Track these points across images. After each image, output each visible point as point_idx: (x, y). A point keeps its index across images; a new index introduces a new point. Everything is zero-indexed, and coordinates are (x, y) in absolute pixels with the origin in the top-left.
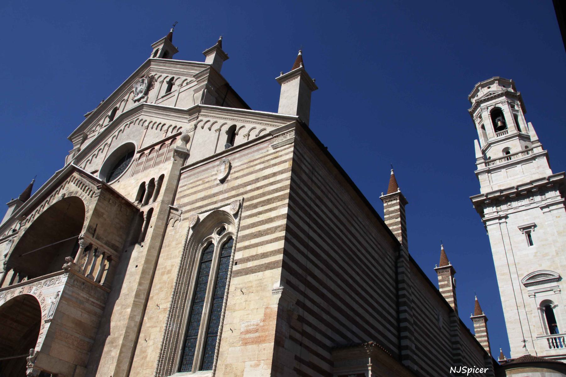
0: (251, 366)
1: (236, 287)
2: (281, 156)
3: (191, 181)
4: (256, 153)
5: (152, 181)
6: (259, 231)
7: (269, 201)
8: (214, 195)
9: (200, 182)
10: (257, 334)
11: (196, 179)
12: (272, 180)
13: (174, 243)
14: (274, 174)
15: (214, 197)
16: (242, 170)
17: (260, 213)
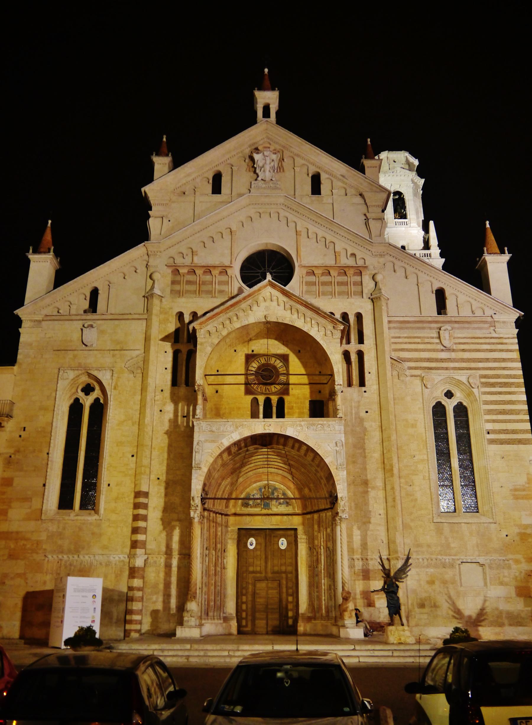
0: (526, 515)
1: (494, 453)
2: (506, 344)
3: (405, 335)
4: (478, 331)
5: (345, 316)
6: (503, 409)
7: (506, 385)
8: (442, 360)
9: (419, 340)
10: (524, 493)
11: (412, 335)
12: (503, 365)
13: (408, 399)
14: (504, 360)
15: (443, 362)
16: (467, 343)
17: (500, 393)
